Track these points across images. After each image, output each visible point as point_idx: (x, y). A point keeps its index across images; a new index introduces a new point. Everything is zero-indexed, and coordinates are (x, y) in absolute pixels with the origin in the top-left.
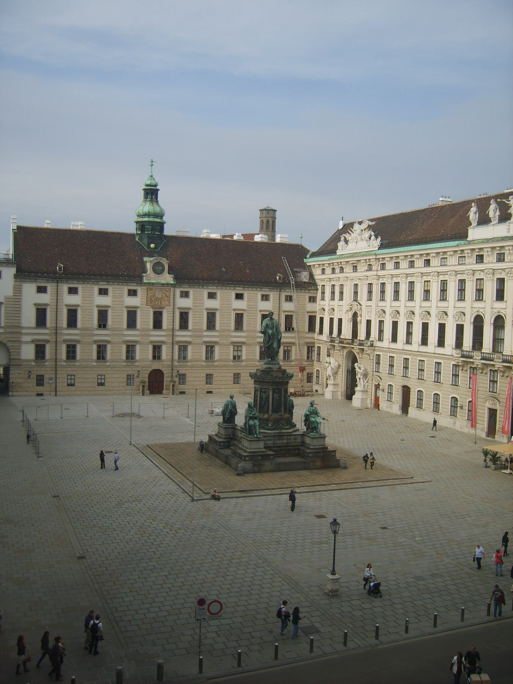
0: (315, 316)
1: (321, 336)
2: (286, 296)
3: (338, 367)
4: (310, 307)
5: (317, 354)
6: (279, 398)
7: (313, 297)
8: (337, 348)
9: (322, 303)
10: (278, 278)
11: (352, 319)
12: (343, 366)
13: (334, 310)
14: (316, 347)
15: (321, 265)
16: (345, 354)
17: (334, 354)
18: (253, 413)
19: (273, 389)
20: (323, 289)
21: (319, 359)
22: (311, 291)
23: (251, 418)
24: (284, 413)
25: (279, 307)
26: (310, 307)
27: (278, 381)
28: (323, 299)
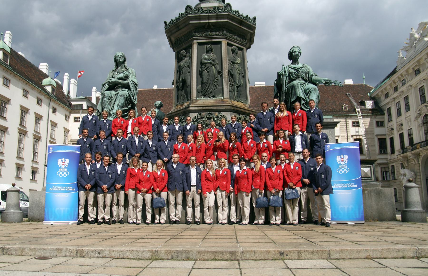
0: (385, 139)
1: (393, 155)
2: (353, 123)
3: (414, 177)
4: (379, 131)
5: (392, 173)
6: (213, 61)
7: (380, 121)
8: (411, 157)
9: (391, 123)
10: (343, 108)
11: (422, 124)
12: (420, 172)
13: (402, 125)
14: (390, 167)
15: (384, 90)
16: (420, 162)
17: (408, 166)
18: (121, 75)
19: (199, 44)
20: (390, 118)
21: (395, 177)
22: (378, 117)
23: (113, 86)
24: (231, 98)
25: (347, 132)
26: (379, 131)
27: (207, 21)
28: (390, 120)
